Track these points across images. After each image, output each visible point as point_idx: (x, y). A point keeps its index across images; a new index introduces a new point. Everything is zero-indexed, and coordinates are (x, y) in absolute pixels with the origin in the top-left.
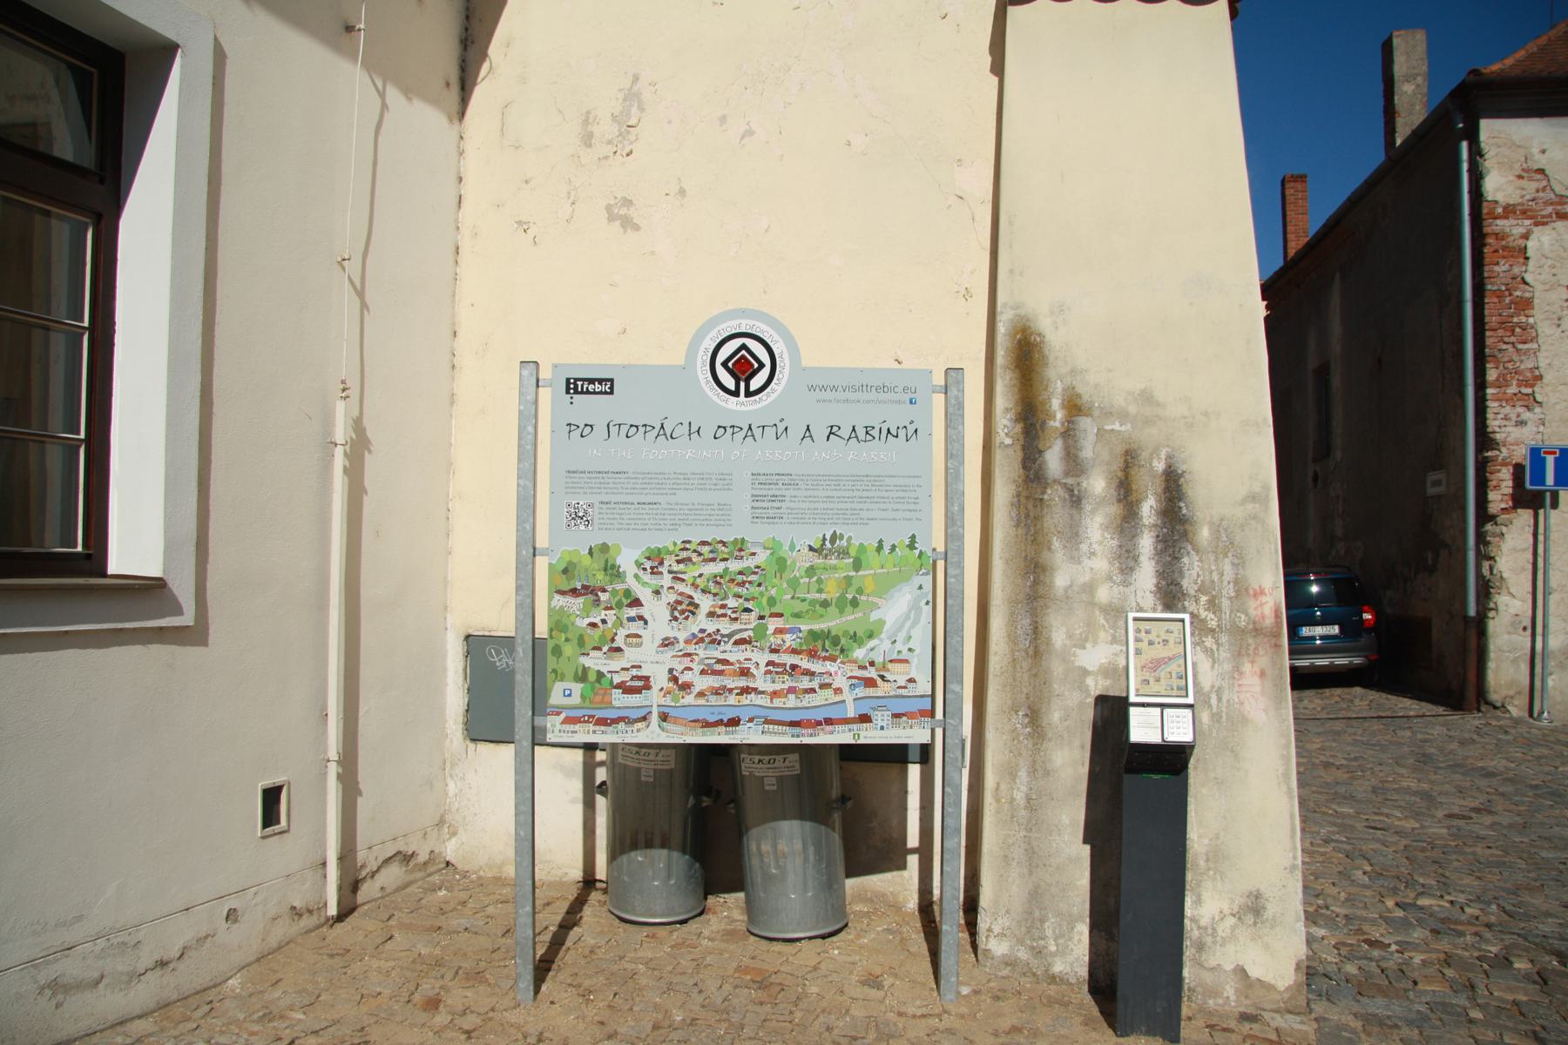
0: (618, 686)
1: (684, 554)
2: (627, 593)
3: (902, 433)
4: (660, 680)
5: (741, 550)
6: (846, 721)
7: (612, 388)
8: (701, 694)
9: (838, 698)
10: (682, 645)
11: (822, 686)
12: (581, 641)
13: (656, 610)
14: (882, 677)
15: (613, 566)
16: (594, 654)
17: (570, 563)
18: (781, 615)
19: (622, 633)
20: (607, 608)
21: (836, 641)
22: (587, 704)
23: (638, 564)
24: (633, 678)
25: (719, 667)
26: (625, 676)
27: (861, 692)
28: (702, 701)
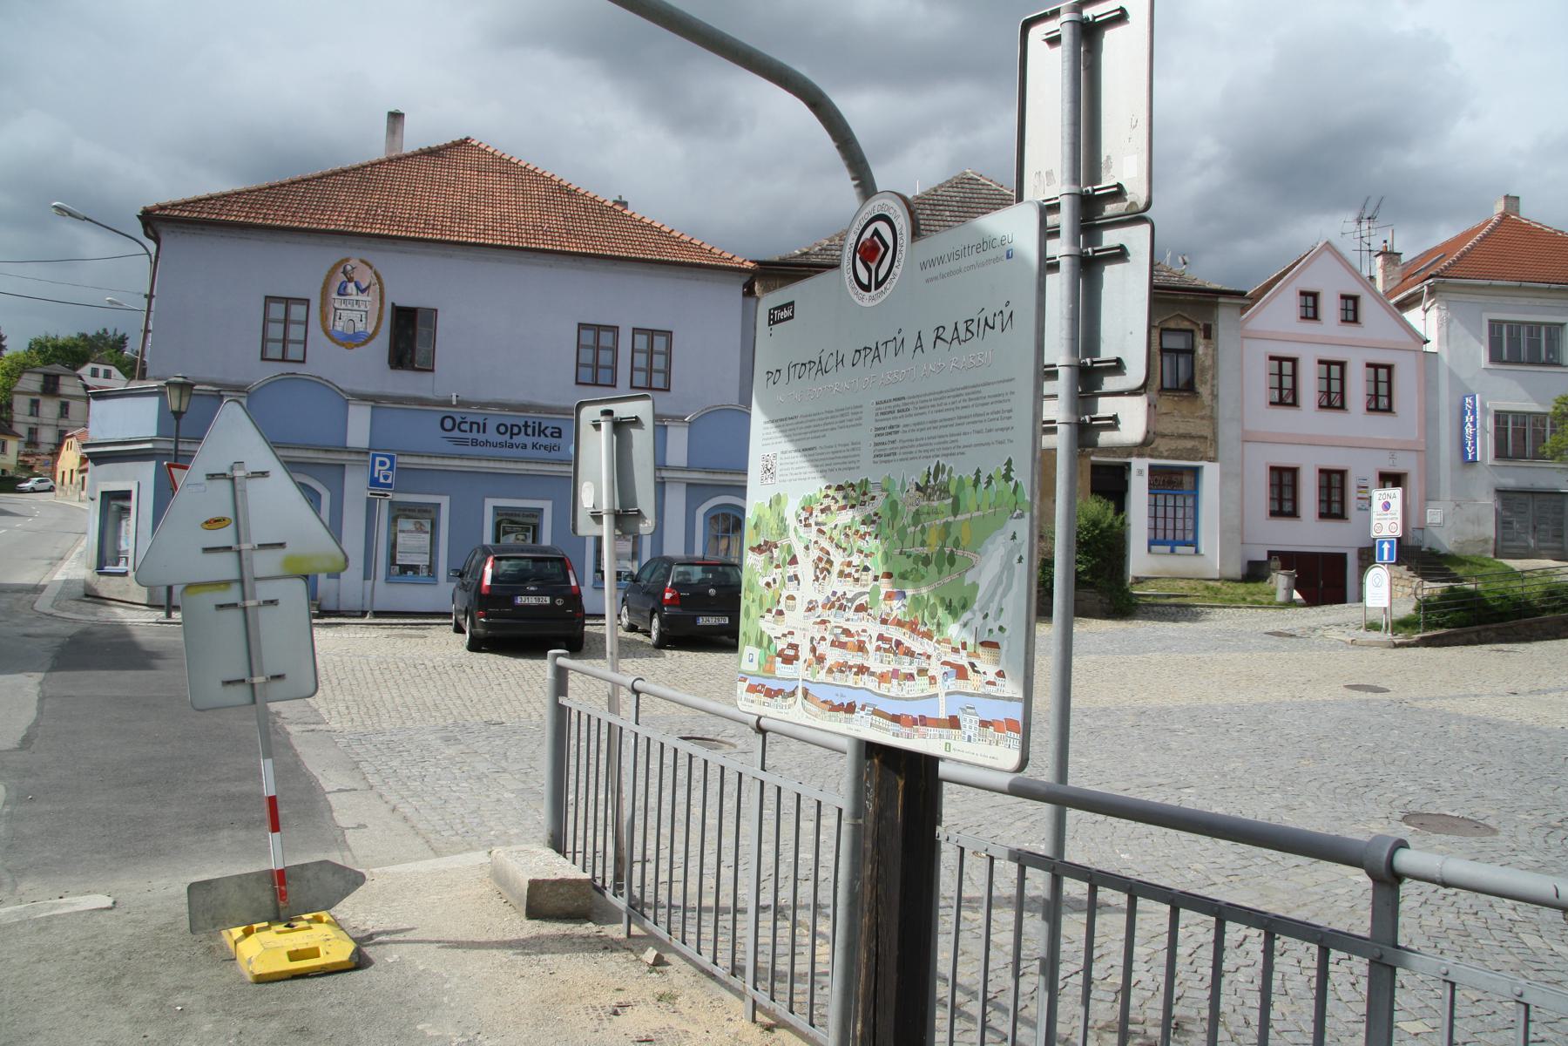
6: (937, 723)
9: (932, 691)
11: (922, 672)
14: (973, 665)
27: (954, 684)
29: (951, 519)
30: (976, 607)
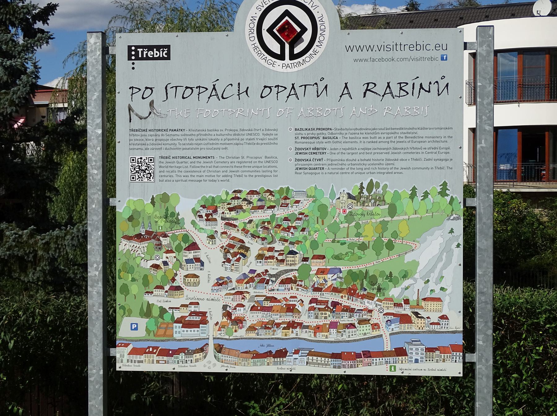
0: (178, 321)
1: (235, 203)
2: (186, 238)
3: (434, 87)
4: (216, 316)
5: (286, 198)
6: (383, 354)
7: (168, 54)
8: (252, 328)
9: (376, 333)
10: (234, 284)
11: (362, 322)
12: (146, 281)
13: (213, 254)
14: (416, 314)
15: (173, 214)
16: (156, 292)
17: (135, 211)
18: (323, 257)
19: (182, 273)
20: (167, 252)
21: (373, 281)
22: (152, 337)
23: (196, 212)
24: (192, 314)
25: (267, 304)
26: (184, 312)
27: (396, 327)
28: (252, 335)
29: (388, 219)
30: (417, 276)
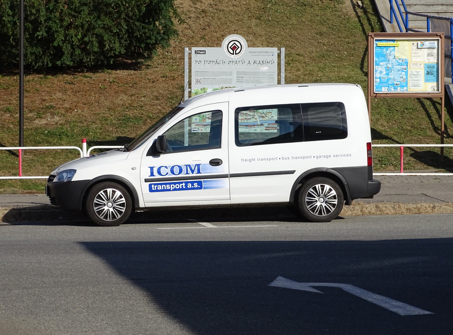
3: (270, 62)
27: (261, 119)
